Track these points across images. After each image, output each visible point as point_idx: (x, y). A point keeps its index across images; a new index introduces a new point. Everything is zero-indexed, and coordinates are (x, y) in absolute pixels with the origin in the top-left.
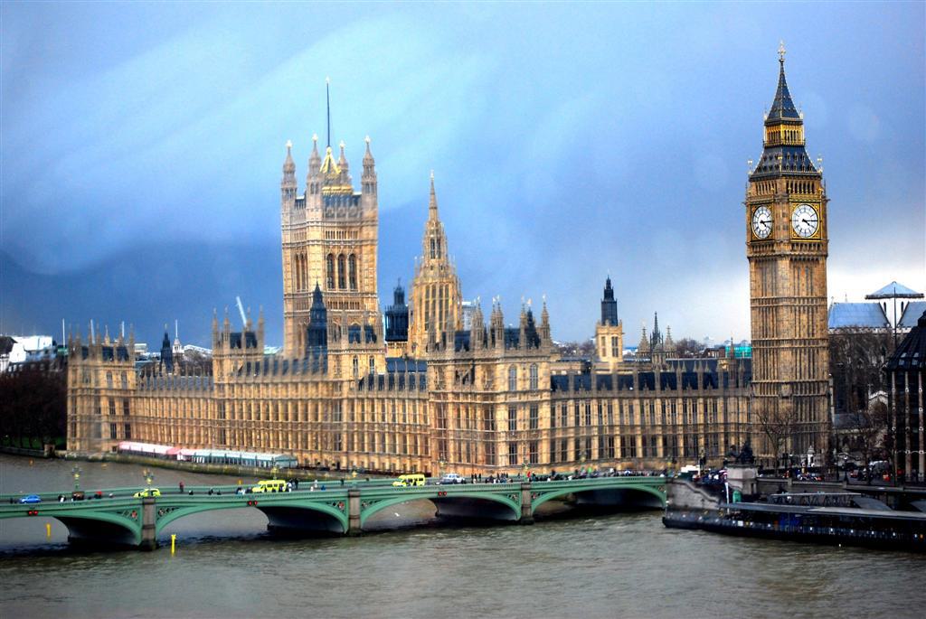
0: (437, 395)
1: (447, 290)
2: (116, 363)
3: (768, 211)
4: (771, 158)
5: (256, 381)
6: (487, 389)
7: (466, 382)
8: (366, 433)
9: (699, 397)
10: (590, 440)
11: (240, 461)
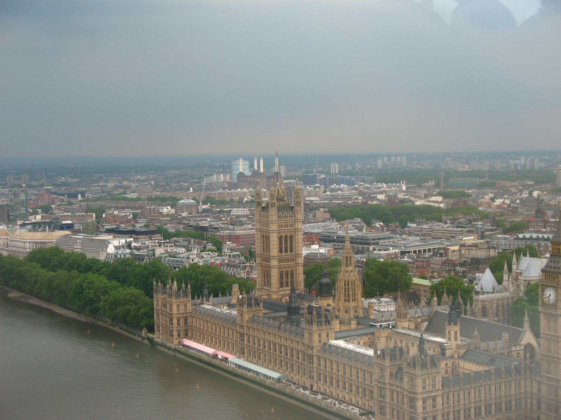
0: (380, 383)
1: (354, 283)
2: (182, 299)
3: (554, 291)
4: (554, 262)
5: (263, 330)
6: (412, 389)
7: (397, 379)
8: (328, 376)
9: (512, 381)
10: (459, 411)
11: (257, 373)
